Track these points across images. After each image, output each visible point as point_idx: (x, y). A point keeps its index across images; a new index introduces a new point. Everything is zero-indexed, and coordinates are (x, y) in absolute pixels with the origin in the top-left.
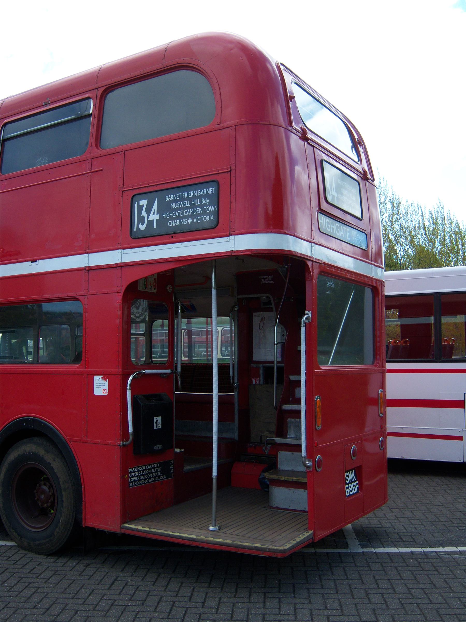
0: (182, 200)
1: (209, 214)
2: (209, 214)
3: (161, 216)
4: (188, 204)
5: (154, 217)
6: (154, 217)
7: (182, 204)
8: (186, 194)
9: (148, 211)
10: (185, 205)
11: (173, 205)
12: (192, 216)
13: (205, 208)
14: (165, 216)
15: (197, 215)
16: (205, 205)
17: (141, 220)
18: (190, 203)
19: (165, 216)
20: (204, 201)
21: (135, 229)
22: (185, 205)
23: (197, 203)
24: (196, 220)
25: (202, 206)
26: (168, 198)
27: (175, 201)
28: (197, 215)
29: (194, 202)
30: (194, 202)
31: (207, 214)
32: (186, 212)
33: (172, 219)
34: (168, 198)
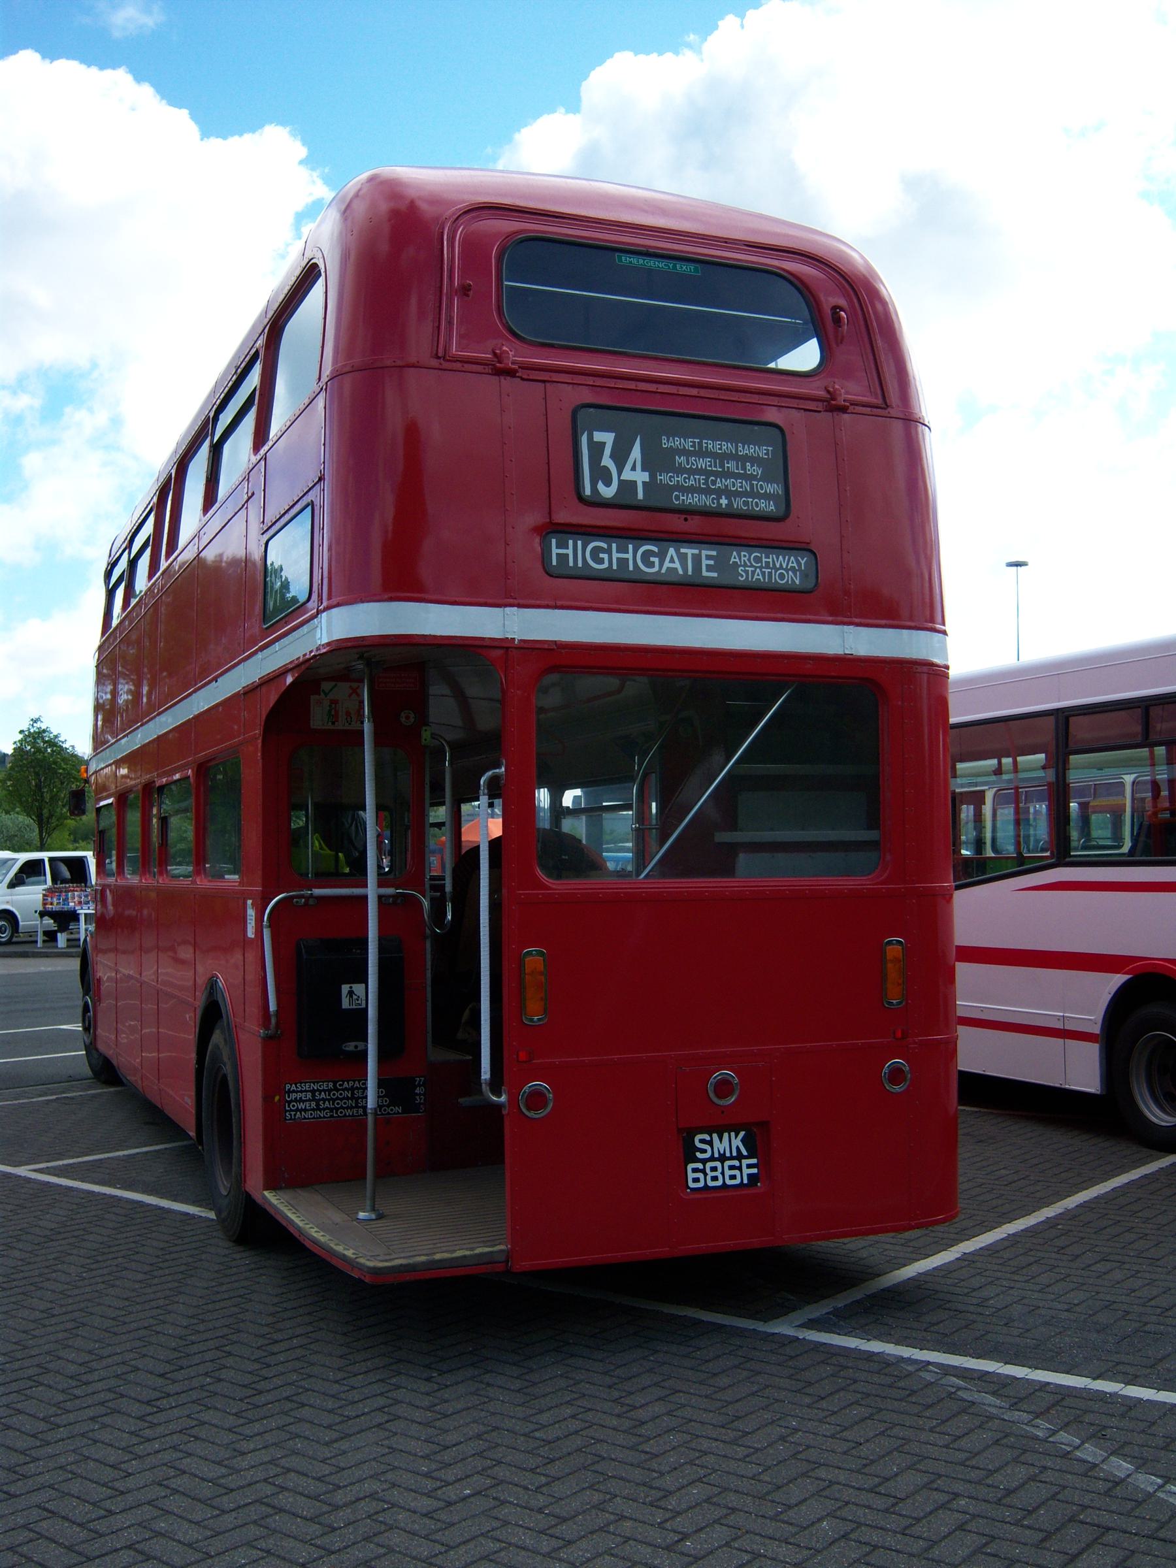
0: (701, 453)
1: (767, 497)
2: (767, 497)
3: (653, 477)
7: (702, 463)
8: (710, 445)
9: (620, 457)
11: (681, 460)
12: (729, 494)
14: (663, 478)
16: (754, 477)
19: (663, 478)
20: (751, 469)
24: (739, 504)
26: (666, 443)
28: (737, 494)
29: (730, 465)
30: (730, 465)
32: (714, 483)
33: (680, 488)
34: (666, 443)
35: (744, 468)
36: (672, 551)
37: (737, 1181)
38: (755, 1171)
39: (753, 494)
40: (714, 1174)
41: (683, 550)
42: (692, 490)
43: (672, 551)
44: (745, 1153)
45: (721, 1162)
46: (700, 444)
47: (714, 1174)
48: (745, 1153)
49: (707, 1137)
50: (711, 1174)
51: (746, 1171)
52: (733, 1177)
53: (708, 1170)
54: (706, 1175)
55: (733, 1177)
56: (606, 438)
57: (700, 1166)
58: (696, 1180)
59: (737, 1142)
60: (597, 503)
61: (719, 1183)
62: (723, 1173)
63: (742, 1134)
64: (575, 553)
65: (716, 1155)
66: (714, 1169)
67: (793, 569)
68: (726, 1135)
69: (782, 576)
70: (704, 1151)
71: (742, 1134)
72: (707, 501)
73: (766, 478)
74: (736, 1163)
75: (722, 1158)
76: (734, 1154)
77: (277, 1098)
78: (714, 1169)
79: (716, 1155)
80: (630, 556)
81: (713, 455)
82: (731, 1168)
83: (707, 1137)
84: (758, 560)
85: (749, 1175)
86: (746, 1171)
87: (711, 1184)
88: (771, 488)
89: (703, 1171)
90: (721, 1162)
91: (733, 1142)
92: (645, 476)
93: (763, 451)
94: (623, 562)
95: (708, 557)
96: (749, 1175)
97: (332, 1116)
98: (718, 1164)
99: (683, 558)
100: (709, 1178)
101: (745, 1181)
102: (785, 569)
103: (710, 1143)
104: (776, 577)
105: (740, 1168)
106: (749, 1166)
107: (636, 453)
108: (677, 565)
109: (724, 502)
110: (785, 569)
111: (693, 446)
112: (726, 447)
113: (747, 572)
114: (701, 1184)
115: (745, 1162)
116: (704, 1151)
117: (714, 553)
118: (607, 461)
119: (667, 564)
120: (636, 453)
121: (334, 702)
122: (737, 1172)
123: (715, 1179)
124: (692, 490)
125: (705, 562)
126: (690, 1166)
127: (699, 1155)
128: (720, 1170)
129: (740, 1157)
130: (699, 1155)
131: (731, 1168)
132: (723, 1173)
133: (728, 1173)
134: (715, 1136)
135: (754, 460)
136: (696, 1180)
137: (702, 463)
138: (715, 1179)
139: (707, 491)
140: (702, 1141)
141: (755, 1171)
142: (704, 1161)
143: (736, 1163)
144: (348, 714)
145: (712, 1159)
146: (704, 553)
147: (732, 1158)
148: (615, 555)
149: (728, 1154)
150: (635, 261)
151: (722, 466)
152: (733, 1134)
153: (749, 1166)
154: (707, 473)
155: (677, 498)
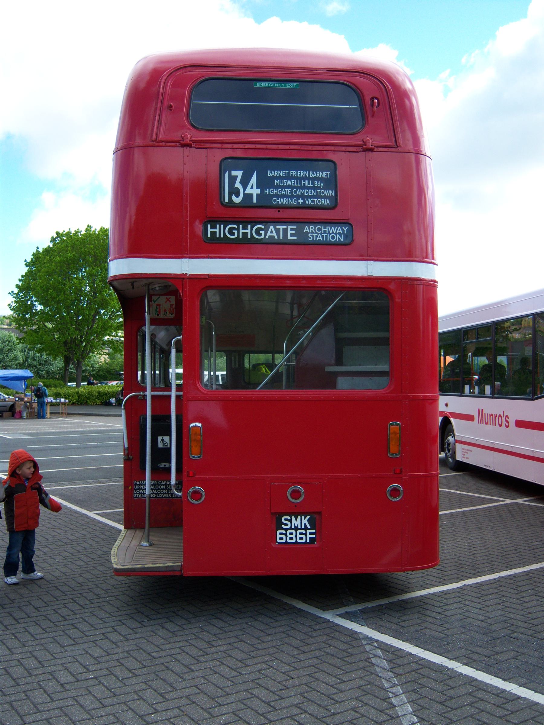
0: (289, 178)
1: (325, 197)
2: (325, 197)
3: (262, 191)
4: (297, 184)
6: (254, 191)
7: (289, 183)
8: (294, 173)
9: (245, 183)
10: (294, 184)
12: (303, 196)
13: (319, 191)
14: (268, 191)
15: (308, 197)
18: (301, 183)
19: (268, 191)
21: (227, 200)
22: (294, 184)
23: (309, 184)
24: (309, 202)
25: (314, 188)
26: (270, 174)
28: (308, 197)
29: (305, 183)
30: (305, 183)
31: (321, 197)
32: (296, 192)
33: (276, 196)
34: (270, 174)
35: (313, 183)
36: (272, 227)
37: (304, 541)
38: (314, 536)
39: (317, 196)
40: (291, 536)
41: (278, 227)
42: (283, 196)
43: (272, 227)
44: (309, 527)
45: (296, 530)
46: (289, 173)
47: (291, 536)
48: (309, 527)
49: (289, 518)
50: (289, 536)
51: (309, 536)
53: (288, 534)
54: (287, 536)
56: (238, 173)
57: (284, 532)
59: (305, 521)
60: (232, 205)
61: (294, 541)
62: (296, 536)
63: (308, 517)
64: (220, 231)
65: (293, 527)
67: (339, 233)
68: (299, 518)
70: (287, 525)
71: (308, 517)
72: (292, 202)
73: (325, 188)
74: (304, 532)
75: (296, 529)
76: (303, 527)
77: (130, 487)
79: (293, 527)
80: (249, 231)
81: (296, 178)
82: (301, 534)
83: (289, 518)
84: (320, 229)
85: (310, 538)
86: (309, 536)
87: (289, 541)
88: (328, 193)
89: (286, 535)
90: (296, 530)
92: (258, 191)
93: (324, 175)
95: (292, 230)
96: (310, 538)
97: (156, 497)
98: (294, 532)
99: (278, 231)
100: (288, 538)
101: (308, 541)
102: (336, 233)
103: (290, 521)
104: (329, 238)
105: (305, 534)
106: (310, 534)
107: (254, 180)
108: (274, 234)
109: (301, 201)
110: (336, 233)
111: (285, 174)
112: (303, 173)
113: (313, 236)
114: (284, 541)
115: (308, 531)
116: (287, 525)
117: (295, 227)
118: (238, 185)
119: (269, 234)
120: (254, 180)
121: (158, 305)
122: (304, 536)
124: (283, 196)
125: (290, 232)
126: (279, 532)
127: (284, 526)
128: (294, 534)
130: (284, 526)
131: (301, 534)
132: (296, 536)
133: (299, 536)
134: (293, 518)
135: (319, 179)
137: (289, 183)
139: (292, 197)
140: (285, 520)
141: (314, 536)
142: (286, 530)
143: (304, 532)
144: (165, 310)
145: (291, 529)
146: (290, 227)
147: (301, 529)
148: (241, 231)
149: (299, 527)
151: (301, 183)
152: (303, 517)
153: (310, 534)
154: (291, 187)
155: (275, 201)
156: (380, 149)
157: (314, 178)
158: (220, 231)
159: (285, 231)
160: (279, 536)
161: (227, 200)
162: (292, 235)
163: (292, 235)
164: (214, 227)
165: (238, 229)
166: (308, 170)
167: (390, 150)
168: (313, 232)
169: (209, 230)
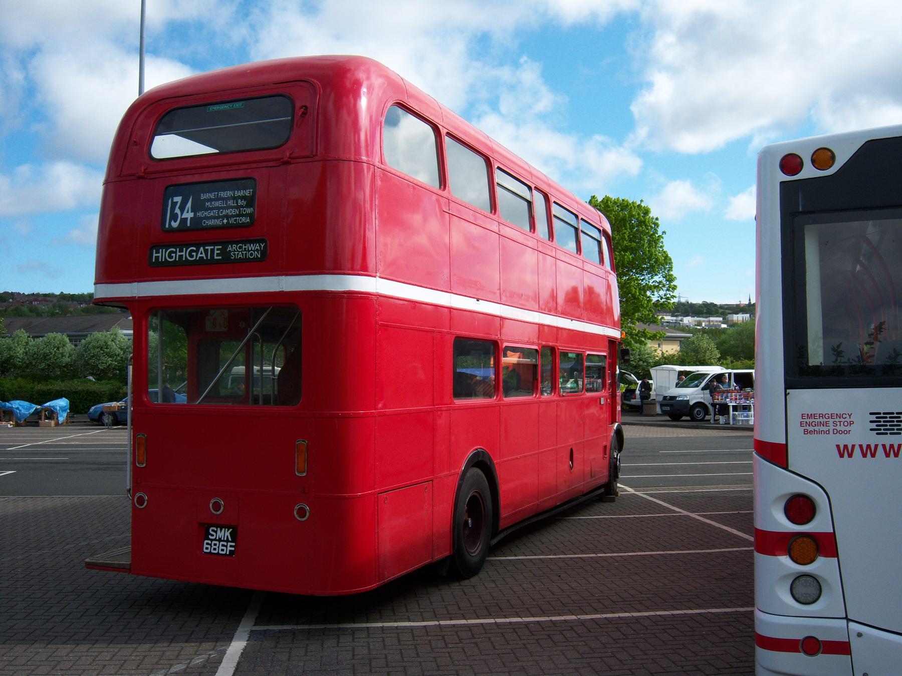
0: (218, 199)
1: (246, 215)
2: (246, 215)
3: (195, 215)
5: (189, 215)
8: (223, 194)
9: (182, 209)
11: (208, 204)
12: (227, 217)
14: (199, 214)
16: (242, 206)
17: (174, 217)
19: (199, 214)
21: (167, 226)
24: (232, 221)
25: (238, 207)
26: (203, 197)
27: (210, 200)
28: (233, 216)
29: (230, 203)
31: (243, 215)
34: (203, 197)
36: (202, 249)
39: (240, 215)
43: (202, 249)
45: (219, 543)
51: (229, 548)
52: (223, 550)
55: (223, 550)
56: (178, 199)
58: (207, 548)
59: (228, 534)
60: (172, 230)
64: (162, 255)
66: (215, 545)
67: (257, 250)
69: (251, 254)
72: (217, 222)
73: (247, 206)
75: (220, 540)
78: (215, 545)
80: (183, 254)
81: (223, 199)
82: (223, 545)
84: (241, 248)
86: (229, 548)
88: (249, 211)
90: (219, 543)
91: (225, 534)
94: (181, 256)
95: (218, 249)
99: (206, 251)
102: (253, 250)
103: (216, 532)
104: (248, 255)
105: (226, 546)
106: (231, 546)
107: (189, 205)
108: (204, 255)
109: (225, 221)
110: (253, 250)
112: (229, 193)
115: (230, 544)
118: (177, 211)
119: (199, 255)
120: (189, 205)
123: (215, 549)
125: (216, 252)
126: (206, 541)
129: (227, 541)
131: (223, 545)
133: (221, 547)
136: (207, 548)
138: (215, 549)
142: (212, 540)
145: (215, 540)
148: (178, 254)
150: (216, 108)
153: (231, 546)
154: (218, 208)
156: (298, 160)
157: (239, 197)
158: (162, 255)
159: (213, 251)
160: (205, 546)
161: (167, 226)
162: (218, 255)
163: (218, 255)
164: (157, 252)
165: (175, 253)
166: (233, 189)
167: (307, 160)
168: (236, 251)
169: (155, 255)
